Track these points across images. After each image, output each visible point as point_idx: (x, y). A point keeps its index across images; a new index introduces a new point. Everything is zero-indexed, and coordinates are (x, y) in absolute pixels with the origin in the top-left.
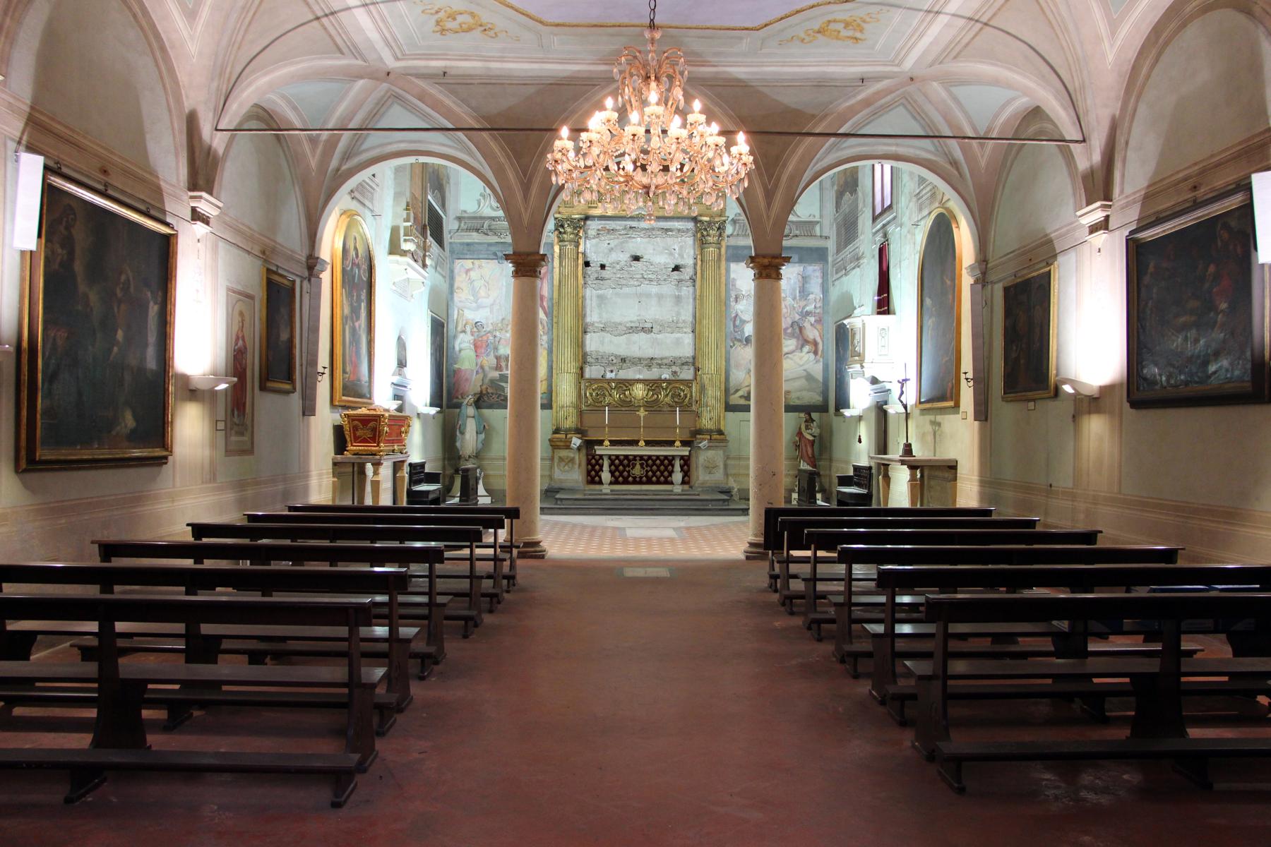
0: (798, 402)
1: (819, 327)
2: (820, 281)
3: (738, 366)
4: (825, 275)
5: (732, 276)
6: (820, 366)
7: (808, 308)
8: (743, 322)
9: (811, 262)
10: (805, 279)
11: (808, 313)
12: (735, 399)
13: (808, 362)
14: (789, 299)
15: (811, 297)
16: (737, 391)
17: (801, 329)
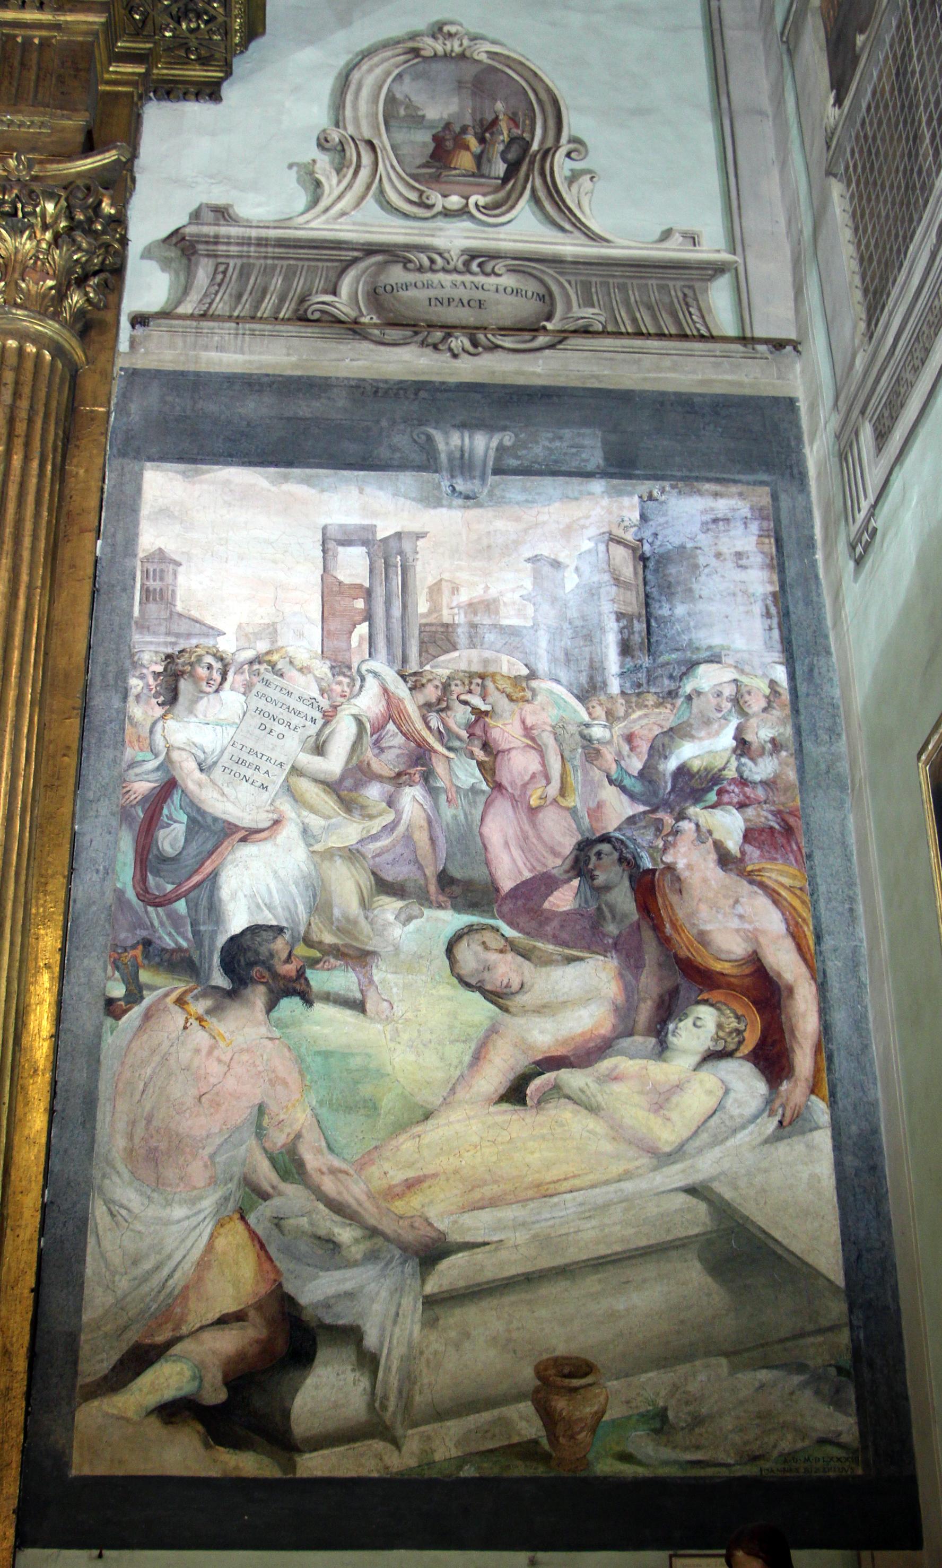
0: (656, 1457)
1: (780, 873)
2: (760, 581)
3: (156, 1157)
4: (787, 551)
5: (150, 538)
6: (812, 1164)
7: (688, 752)
8: (218, 834)
9: (690, 473)
10: (655, 574)
11: (696, 786)
12: (119, 1433)
13: (714, 1125)
14: (555, 701)
15: (707, 678)
16: (140, 1358)
17: (648, 887)
